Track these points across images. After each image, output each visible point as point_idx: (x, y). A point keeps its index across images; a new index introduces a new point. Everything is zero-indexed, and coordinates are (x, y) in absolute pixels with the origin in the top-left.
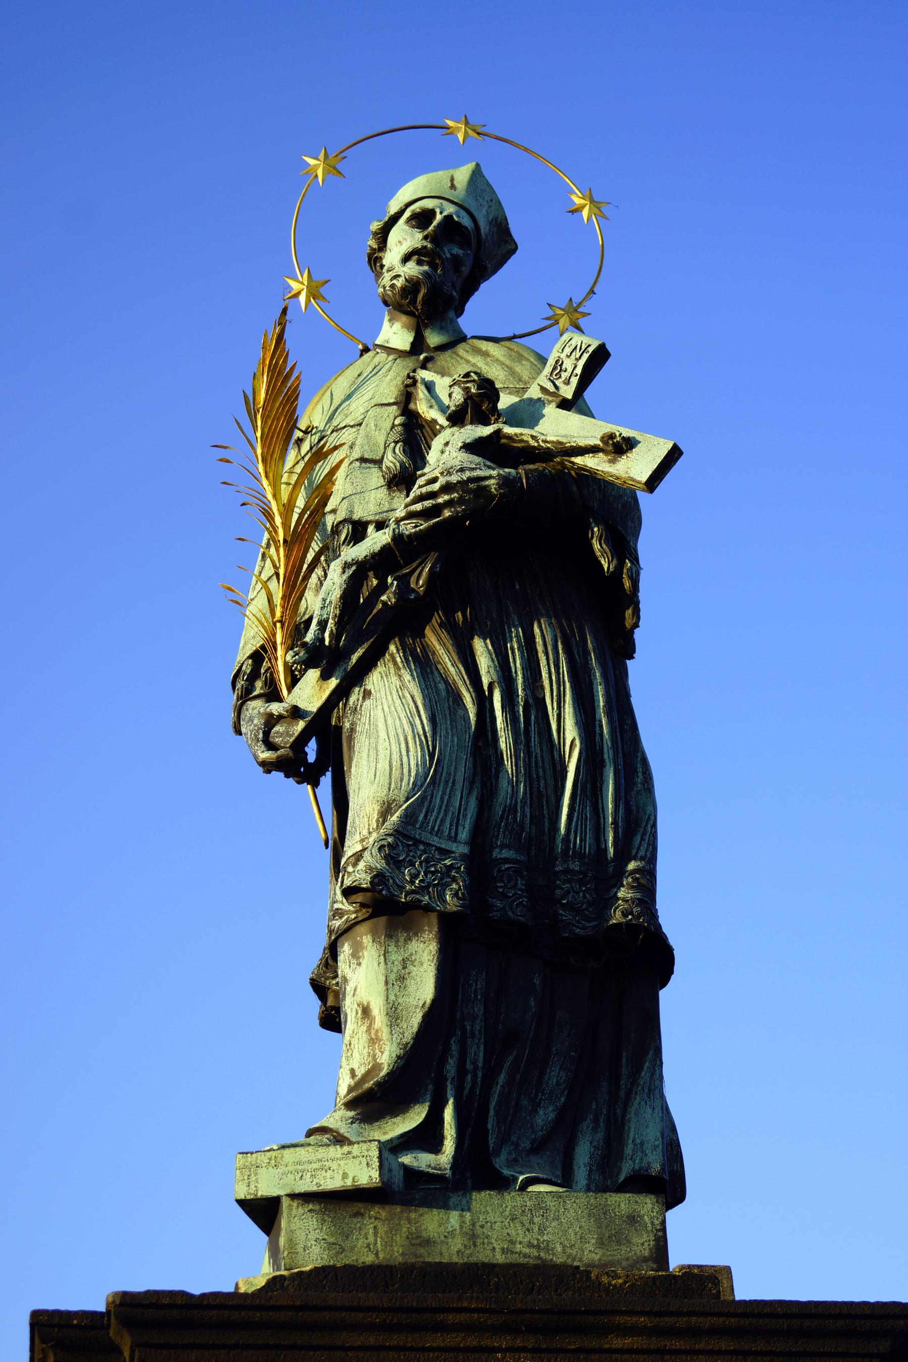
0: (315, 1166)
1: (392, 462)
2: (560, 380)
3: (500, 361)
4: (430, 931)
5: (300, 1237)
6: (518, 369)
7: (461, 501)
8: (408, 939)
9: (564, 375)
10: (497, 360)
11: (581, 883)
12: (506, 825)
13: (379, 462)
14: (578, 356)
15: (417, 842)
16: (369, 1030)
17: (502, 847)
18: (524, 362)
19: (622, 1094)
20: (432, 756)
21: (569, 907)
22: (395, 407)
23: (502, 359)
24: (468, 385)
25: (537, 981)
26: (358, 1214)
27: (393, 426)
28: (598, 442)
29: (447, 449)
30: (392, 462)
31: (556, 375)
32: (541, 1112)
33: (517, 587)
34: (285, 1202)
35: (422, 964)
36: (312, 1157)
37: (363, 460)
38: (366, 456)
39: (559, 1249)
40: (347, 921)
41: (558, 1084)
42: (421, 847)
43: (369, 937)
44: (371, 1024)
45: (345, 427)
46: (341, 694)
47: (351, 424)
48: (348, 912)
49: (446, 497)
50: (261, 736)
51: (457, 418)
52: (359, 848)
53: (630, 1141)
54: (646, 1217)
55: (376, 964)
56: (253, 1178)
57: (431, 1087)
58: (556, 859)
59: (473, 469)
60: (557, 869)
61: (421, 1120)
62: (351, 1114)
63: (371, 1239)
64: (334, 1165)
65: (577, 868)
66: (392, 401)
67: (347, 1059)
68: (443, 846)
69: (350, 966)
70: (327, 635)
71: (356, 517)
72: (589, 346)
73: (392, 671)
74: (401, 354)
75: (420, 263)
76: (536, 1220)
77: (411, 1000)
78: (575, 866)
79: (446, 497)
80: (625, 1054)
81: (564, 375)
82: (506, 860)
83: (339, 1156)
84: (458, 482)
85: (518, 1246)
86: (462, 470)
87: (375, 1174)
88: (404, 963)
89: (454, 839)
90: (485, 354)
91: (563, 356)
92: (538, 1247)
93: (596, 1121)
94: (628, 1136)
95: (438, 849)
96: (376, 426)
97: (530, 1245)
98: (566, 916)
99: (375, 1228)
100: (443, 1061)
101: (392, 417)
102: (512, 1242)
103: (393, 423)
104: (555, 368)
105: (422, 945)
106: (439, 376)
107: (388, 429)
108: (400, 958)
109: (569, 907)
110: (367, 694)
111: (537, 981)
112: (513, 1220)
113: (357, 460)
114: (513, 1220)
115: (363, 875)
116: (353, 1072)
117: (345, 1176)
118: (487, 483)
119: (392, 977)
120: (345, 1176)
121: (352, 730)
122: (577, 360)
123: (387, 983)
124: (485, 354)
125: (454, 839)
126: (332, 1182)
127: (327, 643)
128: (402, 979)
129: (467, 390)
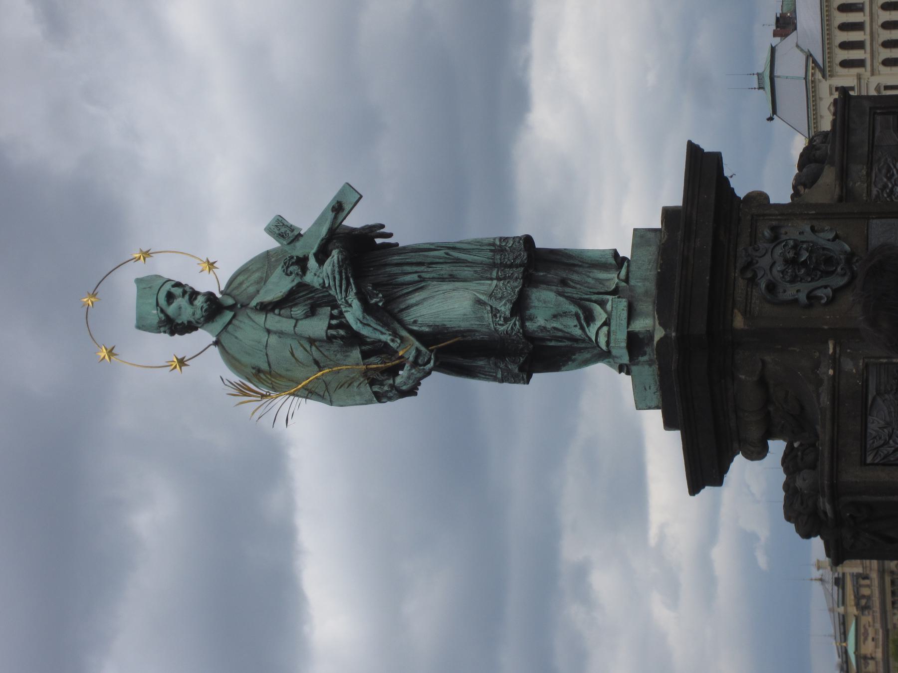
0: (618, 320)
1: (302, 311)
2: (290, 234)
3: (248, 277)
4: (528, 291)
5: (641, 325)
6: (254, 269)
7: (346, 269)
8: (530, 299)
9: (288, 232)
10: (247, 279)
11: (505, 255)
12: (482, 273)
13: (297, 320)
14: (282, 224)
15: (493, 292)
16: (561, 316)
17: (491, 274)
18: (250, 268)
19: (580, 264)
20: (454, 290)
21: (514, 259)
22: (268, 315)
23: (246, 276)
24: (290, 263)
25: (542, 274)
26: (635, 310)
27: (279, 315)
28: (334, 214)
29: (318, 274)
30: (302, 311)
31: (286, 235)
32: (588, 281)
33: (372, 269)
34: (629, 330)
35: (540, 295)
36: (615, 321)
37: (295, 326)
38: (294, 325)
39: (651, 257)
40: (519, 321)
41: (578, 276)
42: (495, 291)
43: (528, 312)
44: (560, 315)
45: (267, 341)
46: (412, 332)
47: (267, 338)
48: (515, 321)
49: (343, 274)
50: (422, 368)
51: (304, 270)
52: (490, 315)
53: (600, 259)
54: (642, 233)
55: (537, 310)
56: (619, 340)
57: (583, 302)
58: (495, 262)
59: (334, 262)
60: (499, 262)
61: (596, 304)
62: (592, 325)
63: (644, 306)
64: (619, 313)
65: (499, 256)
66: (264, 316)
67: (570, 328)
68: (494, 286)
69: (536, 323)
70: (388, 332)
71: (325, 328)
72: (278, 219)
73: (407, 311)
74: (234, 317)
75: (196, 298)
76: (640, 262)
77: (553, 300)
78: (498, 257)
79: (343, 274)
80: (565, 261)
81: (288, 232)
82: (497, 273)
83: (616, 311)
84: (339, 268)
85: (649, 267)
86: (333, 266)
87: (624, 300)
88: (539, 300)
89: (490, 285)
90: (241, 284)
91: (277, 232)
92: (650, 262)
93: (590, 272)
94: (597, 261)
95: (495, 287)
96: (277, 322)
97: (649, 264)
98: (518, 261)
99: (640, 305)
100: (573, 298)
101: (274, 316)
102: (648, 269)
103: (277, 315)
104: (283, 236)
105: (533, 295)
106: (258, 295)
107: (280, 317)
108: (537, 302)
109: (514, 259)
110: (415, 322)
111: (542, 274)
112: (640, 268)
113: (294, 329)
114: (640, 268)
115: (507, 306)
116: (575, 326)
117: (623, 310)
118: (340, 259)
119: (544, 305)
120: (623, 310)
121: (429, 326)
122: (284, 225)
123: (546, 307)
124: (241, 284)
125: (490, 285)
126: (625, 314)
127: (390, 333)
128: (545, 302)
129: (293, 264)
